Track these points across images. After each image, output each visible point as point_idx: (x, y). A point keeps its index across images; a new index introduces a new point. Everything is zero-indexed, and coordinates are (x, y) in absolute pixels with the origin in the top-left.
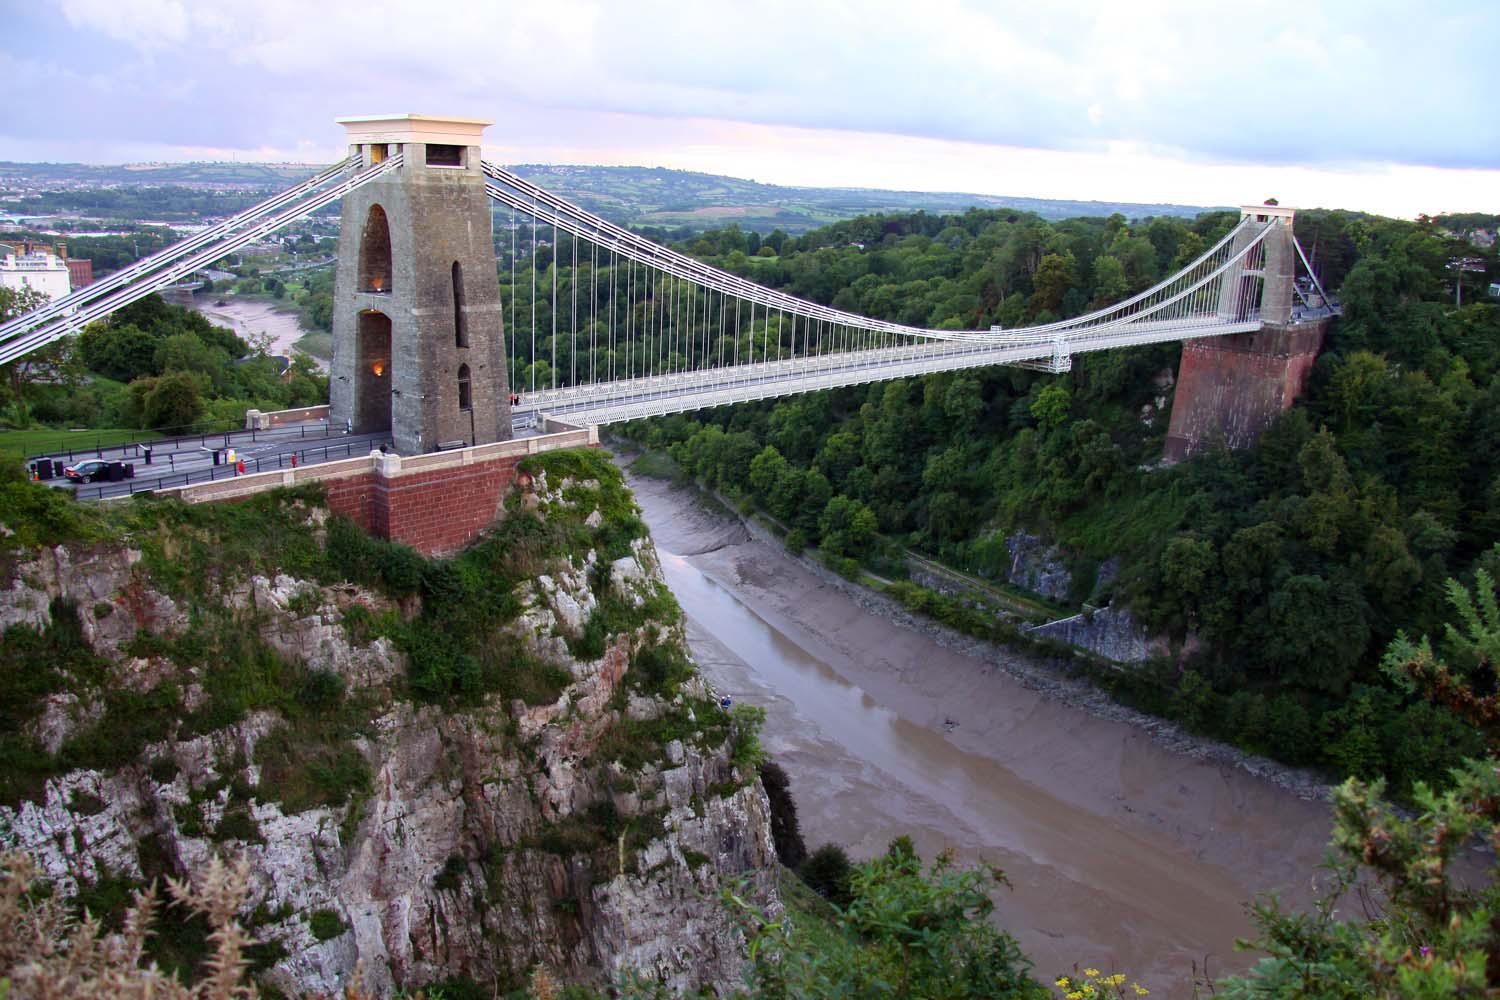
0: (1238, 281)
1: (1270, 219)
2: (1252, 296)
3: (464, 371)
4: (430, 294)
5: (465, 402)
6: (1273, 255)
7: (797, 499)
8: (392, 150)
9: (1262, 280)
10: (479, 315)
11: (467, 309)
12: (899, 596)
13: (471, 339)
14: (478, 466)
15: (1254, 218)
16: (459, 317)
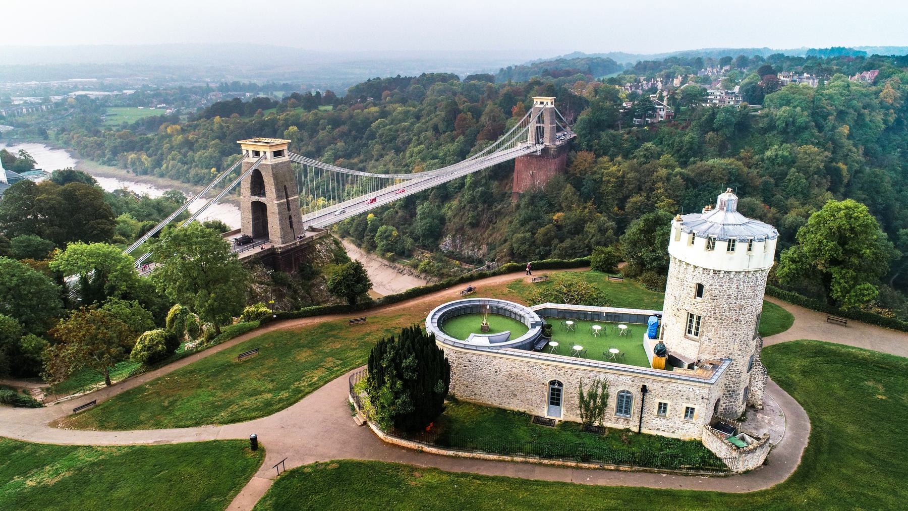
0: (534, 128)
1: (545, 103)
2: (540, 132)
3: (290, 217)
4: (279, 197)
5: (291, 227)
6: (547, 118)
7: (364, 230)
8: (262, 154)
9: (543, 128)
10: (292, 200)
11: (290, 199)
12: (415, 266)
13: (291, 207)
14: (301, 246)
15: (539, 103)
16: (288, 201)
